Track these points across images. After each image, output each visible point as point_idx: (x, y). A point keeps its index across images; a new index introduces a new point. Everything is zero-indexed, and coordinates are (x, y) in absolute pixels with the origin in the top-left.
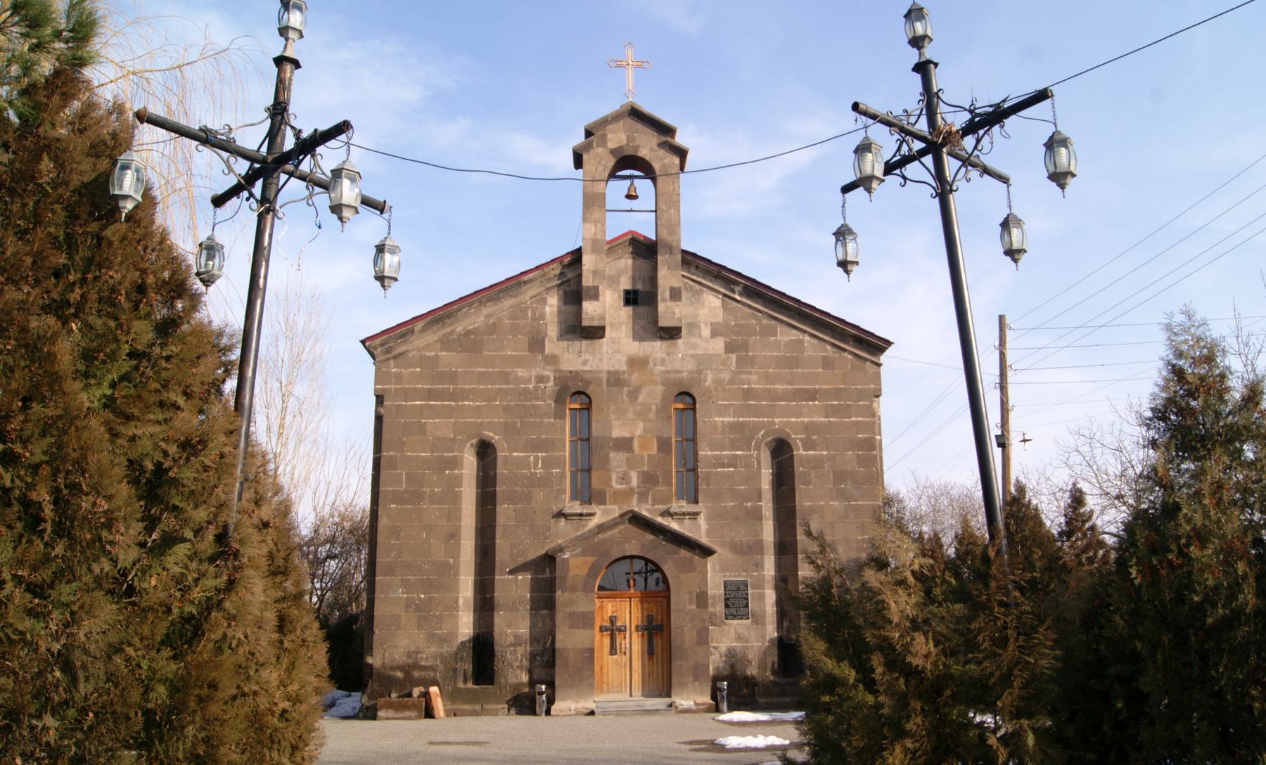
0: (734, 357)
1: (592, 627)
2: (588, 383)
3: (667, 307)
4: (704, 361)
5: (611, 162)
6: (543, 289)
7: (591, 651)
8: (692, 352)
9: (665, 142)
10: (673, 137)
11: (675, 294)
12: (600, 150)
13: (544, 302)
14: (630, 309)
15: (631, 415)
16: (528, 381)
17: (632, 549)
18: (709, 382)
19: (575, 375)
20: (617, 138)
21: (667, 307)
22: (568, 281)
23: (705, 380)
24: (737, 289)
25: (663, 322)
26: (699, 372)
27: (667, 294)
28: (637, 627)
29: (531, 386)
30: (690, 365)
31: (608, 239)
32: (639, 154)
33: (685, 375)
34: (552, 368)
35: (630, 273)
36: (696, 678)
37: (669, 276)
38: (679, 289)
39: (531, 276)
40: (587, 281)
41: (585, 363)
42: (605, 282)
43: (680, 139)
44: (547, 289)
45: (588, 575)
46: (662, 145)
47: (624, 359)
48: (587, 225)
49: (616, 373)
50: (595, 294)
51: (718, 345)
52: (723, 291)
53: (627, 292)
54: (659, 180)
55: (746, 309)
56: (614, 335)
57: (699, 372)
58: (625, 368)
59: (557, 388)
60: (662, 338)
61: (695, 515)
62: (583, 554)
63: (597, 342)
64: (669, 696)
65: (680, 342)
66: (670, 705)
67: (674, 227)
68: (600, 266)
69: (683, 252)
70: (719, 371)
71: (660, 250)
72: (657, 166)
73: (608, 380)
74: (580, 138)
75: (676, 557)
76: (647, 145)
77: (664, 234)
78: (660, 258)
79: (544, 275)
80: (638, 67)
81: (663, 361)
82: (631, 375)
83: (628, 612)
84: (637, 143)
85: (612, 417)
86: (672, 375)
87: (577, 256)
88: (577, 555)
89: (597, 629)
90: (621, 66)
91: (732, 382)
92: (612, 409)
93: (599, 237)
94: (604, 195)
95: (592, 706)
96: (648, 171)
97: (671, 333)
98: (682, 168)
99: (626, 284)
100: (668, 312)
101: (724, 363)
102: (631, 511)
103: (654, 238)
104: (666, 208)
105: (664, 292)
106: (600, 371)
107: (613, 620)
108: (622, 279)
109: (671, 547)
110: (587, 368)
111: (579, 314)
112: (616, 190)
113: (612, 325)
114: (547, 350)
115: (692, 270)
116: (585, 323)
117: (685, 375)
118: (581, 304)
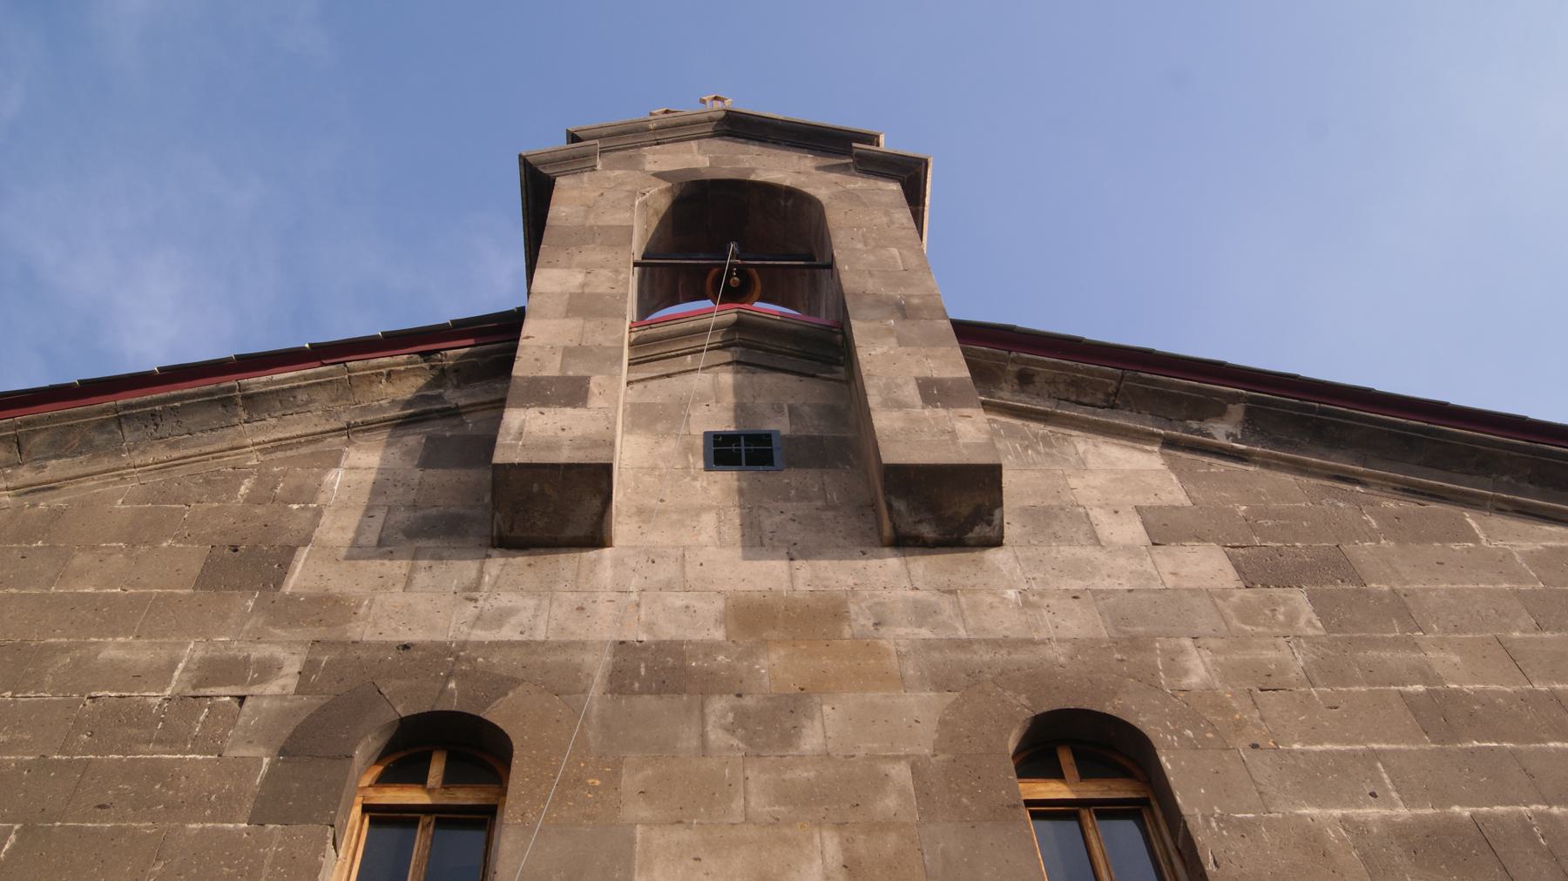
2: (502, 684)
14: (727, 479)
15: (755, 792)
58: (719, 635)
85: (636, 811)
86: (984, 656)
92: (630, 781)
110: (508, 633)
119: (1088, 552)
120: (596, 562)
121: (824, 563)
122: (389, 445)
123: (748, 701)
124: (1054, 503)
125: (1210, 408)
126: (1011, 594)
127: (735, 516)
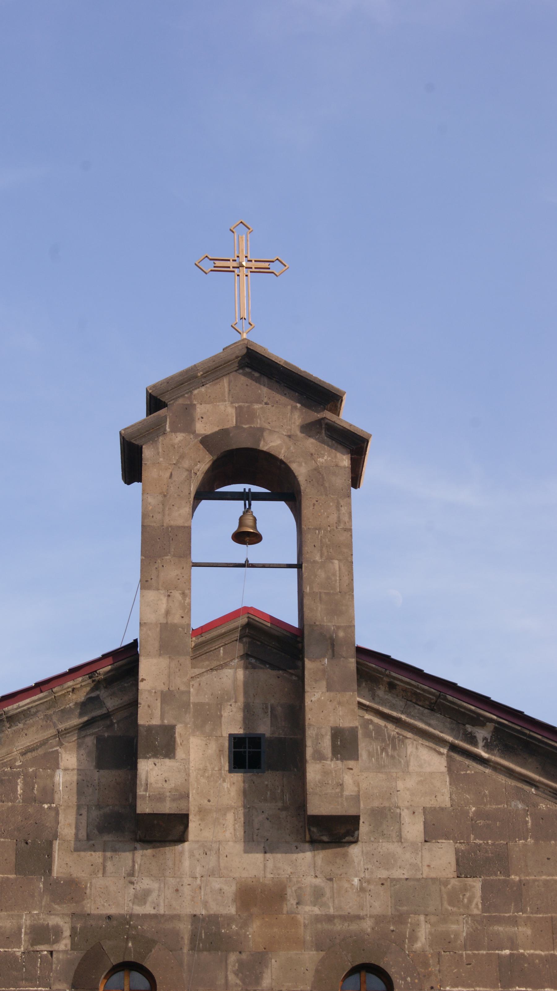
0: (477, 884)
2: (148, 944)
3: (326, 773)
4: (409, 895)
5: (203, 463)
6: (52, 731)
8: (383, 874)
9: (319, 422)
10: (336, 410)
11: (344, 744)
12: (179, 437)
13: (52, 762)
14: (238, 777)
16: (12, 938)
18: (422, 941)
19: (120, 925)
20: (216, 412)
21: (326, 773)
22: (107, 716)
23: (413, 938)
24: (481, 734)
25: (317, 807)
26: (400, 918)
27: (326, 743)
29: (18, 951)
30: (378, 904)
31: (196, 624)
32: (264, 447)
33: (367, 925)
34: (66, 908)
35: (241, 699)
37: (329, 706)
38: (353, 731)
39: (24, 703)
40: (149, 715)
41: (142, 897)
42: (189, 718)
43: (350, 416)
44: (61, 734)
46: (309, 429)
47: (230, 890)
48: (151, 595)
49: (213, 920)
50: (165, 744)
51: (441, 859)
52: (450, 739)
53: (236, 742)
54: (307, 510)
55: (502, 779)
56: (207, 834)
57: (400, 918)
58: (232, 910)
59: (78, 955)
60: (315, 843)
63: (170, 852)
65: (355, 851)
67: (341, 598)
68: (179, 683)
69: (361, 652)
70: (445, 918)
71: (310, 648)
72: (301, 471)
73: (194, 937)
74: (136, 413)
76: (281, 430)
77: (318, 614)
78: (309, 665)
79: (55, 701)
80: (259, 271)
81: (318, 895)
82: (245, 924)
84: (258, 423)
86: (339, 926)
87: (124, 663)
90: (226, 270)
91: (473, 941)
93: (176, 619)
94: (189, 528)
96: (282, 485)
97: (336, 832)
98: (356, 482)
99: (232, 723)
100: (330, 783)
101: (454, 898)
103: (295, 623)
104: (322, 561)
105: (319, 737)
106: (176, 917)
108: (226, 713)
110: (148, 909)
111: (129, 787)
112: (216, 519)
113: (201, 811)
114: (57, 869)
115: (381, 692)
116: (144, 807)
117: (367, 925)
118: (134, 767)
119: (393, 847)
120: (182, 853)
121: (279, 856)
122: (79, 746)
123: (244, 956)
124: (386, 804)
125: (479, 721)
126: (356, 881)
127: (241, 811)
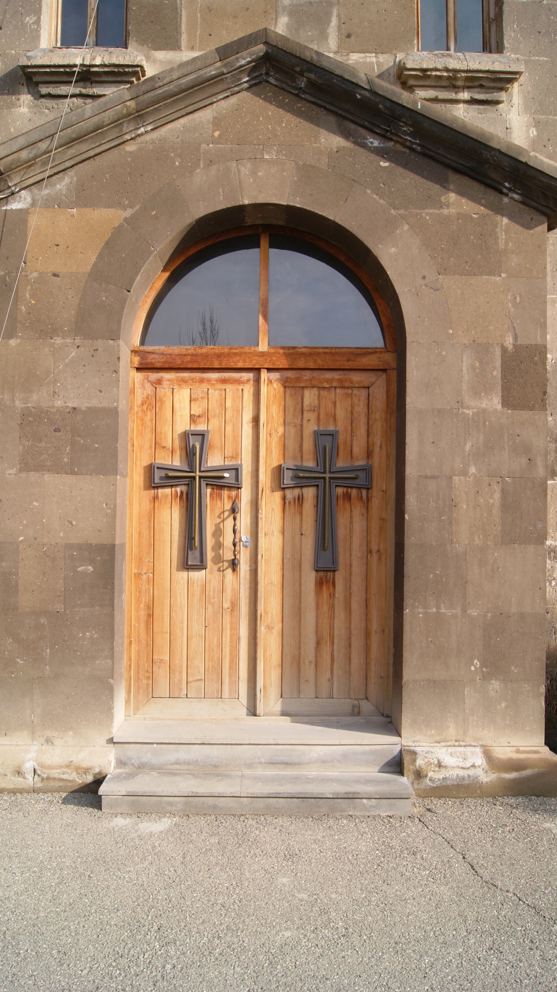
1: (108, 464)
7: (105, 558)
17: (265, 183)
28: (279, 471)
36: (495, 665)
45: (97, 275)
61: (501, 81)
62: (82, 197)
64: (390, 724)
66: (397, 765)
75: (428, 214)
83: (248, 424)
88: (50, 203)
89: (138, 477)
95: (103, 759)
102: (262, 36)
107: (193, 445)
109: (409, 181)
